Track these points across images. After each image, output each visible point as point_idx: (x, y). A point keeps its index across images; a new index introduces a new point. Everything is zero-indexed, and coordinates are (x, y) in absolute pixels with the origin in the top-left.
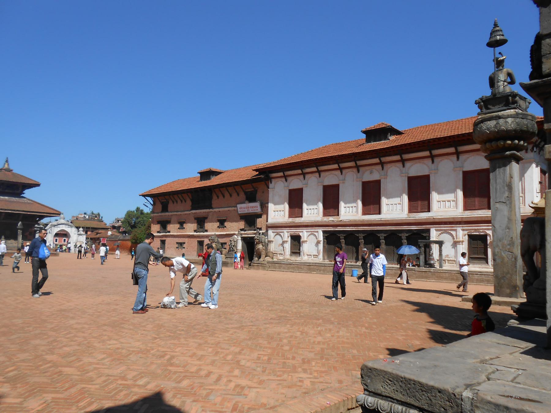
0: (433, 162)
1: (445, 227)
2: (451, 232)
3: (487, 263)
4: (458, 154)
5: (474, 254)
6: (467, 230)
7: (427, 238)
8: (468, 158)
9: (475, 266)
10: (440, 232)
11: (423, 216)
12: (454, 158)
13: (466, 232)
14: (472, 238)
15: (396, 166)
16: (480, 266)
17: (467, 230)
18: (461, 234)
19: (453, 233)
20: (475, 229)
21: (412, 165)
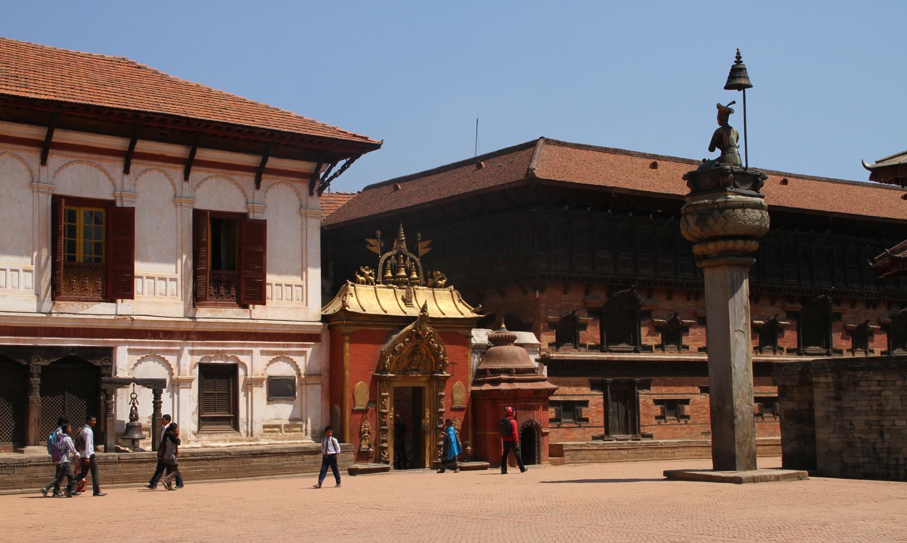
0: (126, 171)
1: (153, 344)
2: (167, 357)
3: (236, 427)
4: (189, 164)
5: (208, 410)
6: (200, 352)
7: (104, 371)
8: (206, 179)
9: (215, 437)
10: (139, 357)
11: (101, 311)
12: (177, 172)
13: (197, 359)
14: (207, 371)
15: (15, 156)
16: (223, 436)
17: (200, 352)
18: (187, 362)
19: (172, 359)
20: (218, 352)
21: (67, 165)
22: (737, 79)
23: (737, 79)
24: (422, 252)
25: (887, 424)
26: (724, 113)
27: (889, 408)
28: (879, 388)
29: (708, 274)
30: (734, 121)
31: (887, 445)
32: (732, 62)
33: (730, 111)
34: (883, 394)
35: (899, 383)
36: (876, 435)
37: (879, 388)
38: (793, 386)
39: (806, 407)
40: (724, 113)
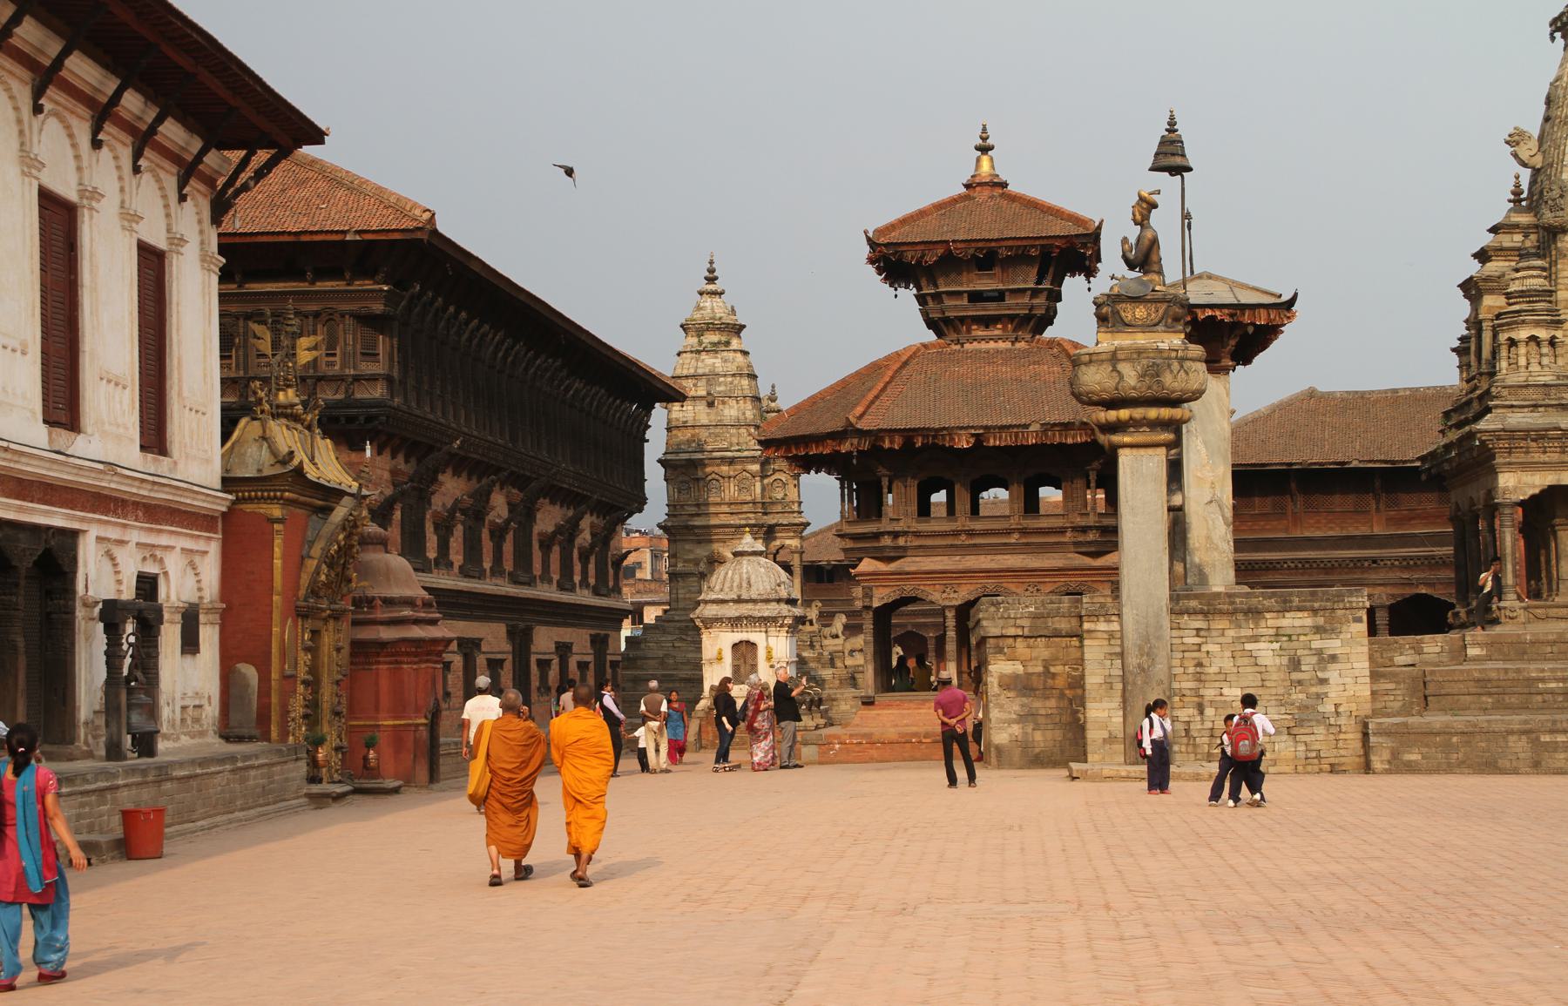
22: (1171, 158)
23: (1171, 158)
24: (304, 357)
25: (1209, 693)
26: (1146, 206)
27: (1212, 670)
28: (1197, 640)
29: (1125, 459)
30: (1164, 223)
31: (1209, 725)
32: (1161, 130)
33: (1155, 206)
34: (1204, 648)
35: (1231, 633)
36: (1191, 711)
37: (1197, 640)
38: (1015, 637)
39: (1040, 669)
40: (1146, 206)
